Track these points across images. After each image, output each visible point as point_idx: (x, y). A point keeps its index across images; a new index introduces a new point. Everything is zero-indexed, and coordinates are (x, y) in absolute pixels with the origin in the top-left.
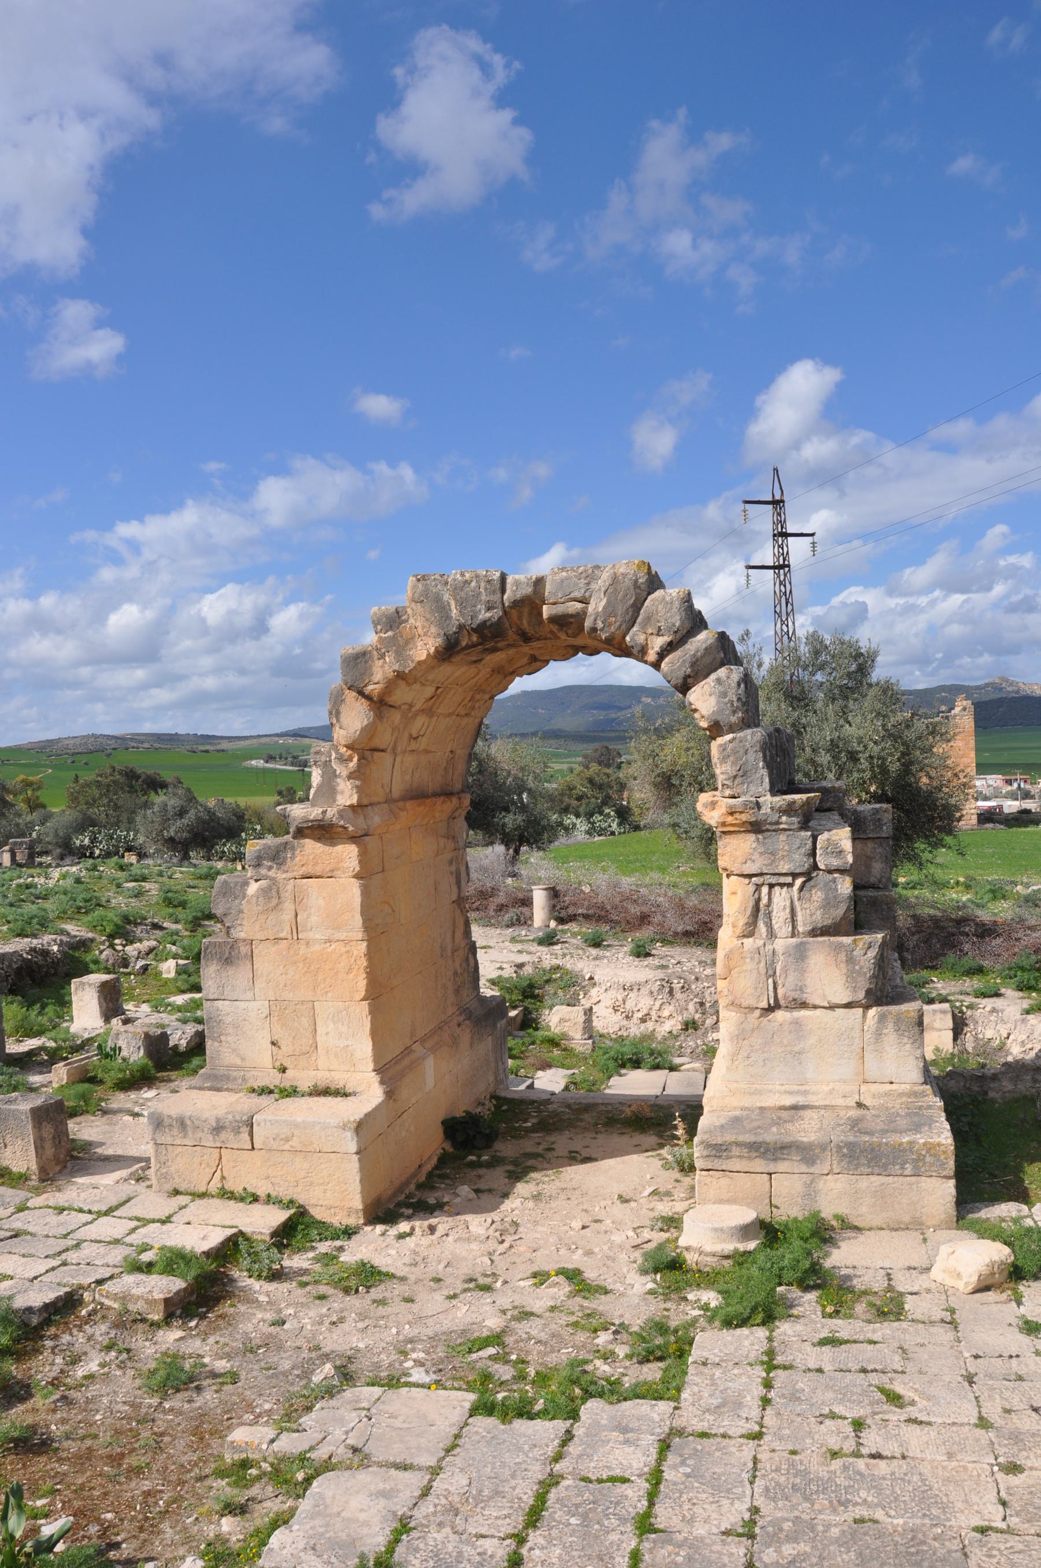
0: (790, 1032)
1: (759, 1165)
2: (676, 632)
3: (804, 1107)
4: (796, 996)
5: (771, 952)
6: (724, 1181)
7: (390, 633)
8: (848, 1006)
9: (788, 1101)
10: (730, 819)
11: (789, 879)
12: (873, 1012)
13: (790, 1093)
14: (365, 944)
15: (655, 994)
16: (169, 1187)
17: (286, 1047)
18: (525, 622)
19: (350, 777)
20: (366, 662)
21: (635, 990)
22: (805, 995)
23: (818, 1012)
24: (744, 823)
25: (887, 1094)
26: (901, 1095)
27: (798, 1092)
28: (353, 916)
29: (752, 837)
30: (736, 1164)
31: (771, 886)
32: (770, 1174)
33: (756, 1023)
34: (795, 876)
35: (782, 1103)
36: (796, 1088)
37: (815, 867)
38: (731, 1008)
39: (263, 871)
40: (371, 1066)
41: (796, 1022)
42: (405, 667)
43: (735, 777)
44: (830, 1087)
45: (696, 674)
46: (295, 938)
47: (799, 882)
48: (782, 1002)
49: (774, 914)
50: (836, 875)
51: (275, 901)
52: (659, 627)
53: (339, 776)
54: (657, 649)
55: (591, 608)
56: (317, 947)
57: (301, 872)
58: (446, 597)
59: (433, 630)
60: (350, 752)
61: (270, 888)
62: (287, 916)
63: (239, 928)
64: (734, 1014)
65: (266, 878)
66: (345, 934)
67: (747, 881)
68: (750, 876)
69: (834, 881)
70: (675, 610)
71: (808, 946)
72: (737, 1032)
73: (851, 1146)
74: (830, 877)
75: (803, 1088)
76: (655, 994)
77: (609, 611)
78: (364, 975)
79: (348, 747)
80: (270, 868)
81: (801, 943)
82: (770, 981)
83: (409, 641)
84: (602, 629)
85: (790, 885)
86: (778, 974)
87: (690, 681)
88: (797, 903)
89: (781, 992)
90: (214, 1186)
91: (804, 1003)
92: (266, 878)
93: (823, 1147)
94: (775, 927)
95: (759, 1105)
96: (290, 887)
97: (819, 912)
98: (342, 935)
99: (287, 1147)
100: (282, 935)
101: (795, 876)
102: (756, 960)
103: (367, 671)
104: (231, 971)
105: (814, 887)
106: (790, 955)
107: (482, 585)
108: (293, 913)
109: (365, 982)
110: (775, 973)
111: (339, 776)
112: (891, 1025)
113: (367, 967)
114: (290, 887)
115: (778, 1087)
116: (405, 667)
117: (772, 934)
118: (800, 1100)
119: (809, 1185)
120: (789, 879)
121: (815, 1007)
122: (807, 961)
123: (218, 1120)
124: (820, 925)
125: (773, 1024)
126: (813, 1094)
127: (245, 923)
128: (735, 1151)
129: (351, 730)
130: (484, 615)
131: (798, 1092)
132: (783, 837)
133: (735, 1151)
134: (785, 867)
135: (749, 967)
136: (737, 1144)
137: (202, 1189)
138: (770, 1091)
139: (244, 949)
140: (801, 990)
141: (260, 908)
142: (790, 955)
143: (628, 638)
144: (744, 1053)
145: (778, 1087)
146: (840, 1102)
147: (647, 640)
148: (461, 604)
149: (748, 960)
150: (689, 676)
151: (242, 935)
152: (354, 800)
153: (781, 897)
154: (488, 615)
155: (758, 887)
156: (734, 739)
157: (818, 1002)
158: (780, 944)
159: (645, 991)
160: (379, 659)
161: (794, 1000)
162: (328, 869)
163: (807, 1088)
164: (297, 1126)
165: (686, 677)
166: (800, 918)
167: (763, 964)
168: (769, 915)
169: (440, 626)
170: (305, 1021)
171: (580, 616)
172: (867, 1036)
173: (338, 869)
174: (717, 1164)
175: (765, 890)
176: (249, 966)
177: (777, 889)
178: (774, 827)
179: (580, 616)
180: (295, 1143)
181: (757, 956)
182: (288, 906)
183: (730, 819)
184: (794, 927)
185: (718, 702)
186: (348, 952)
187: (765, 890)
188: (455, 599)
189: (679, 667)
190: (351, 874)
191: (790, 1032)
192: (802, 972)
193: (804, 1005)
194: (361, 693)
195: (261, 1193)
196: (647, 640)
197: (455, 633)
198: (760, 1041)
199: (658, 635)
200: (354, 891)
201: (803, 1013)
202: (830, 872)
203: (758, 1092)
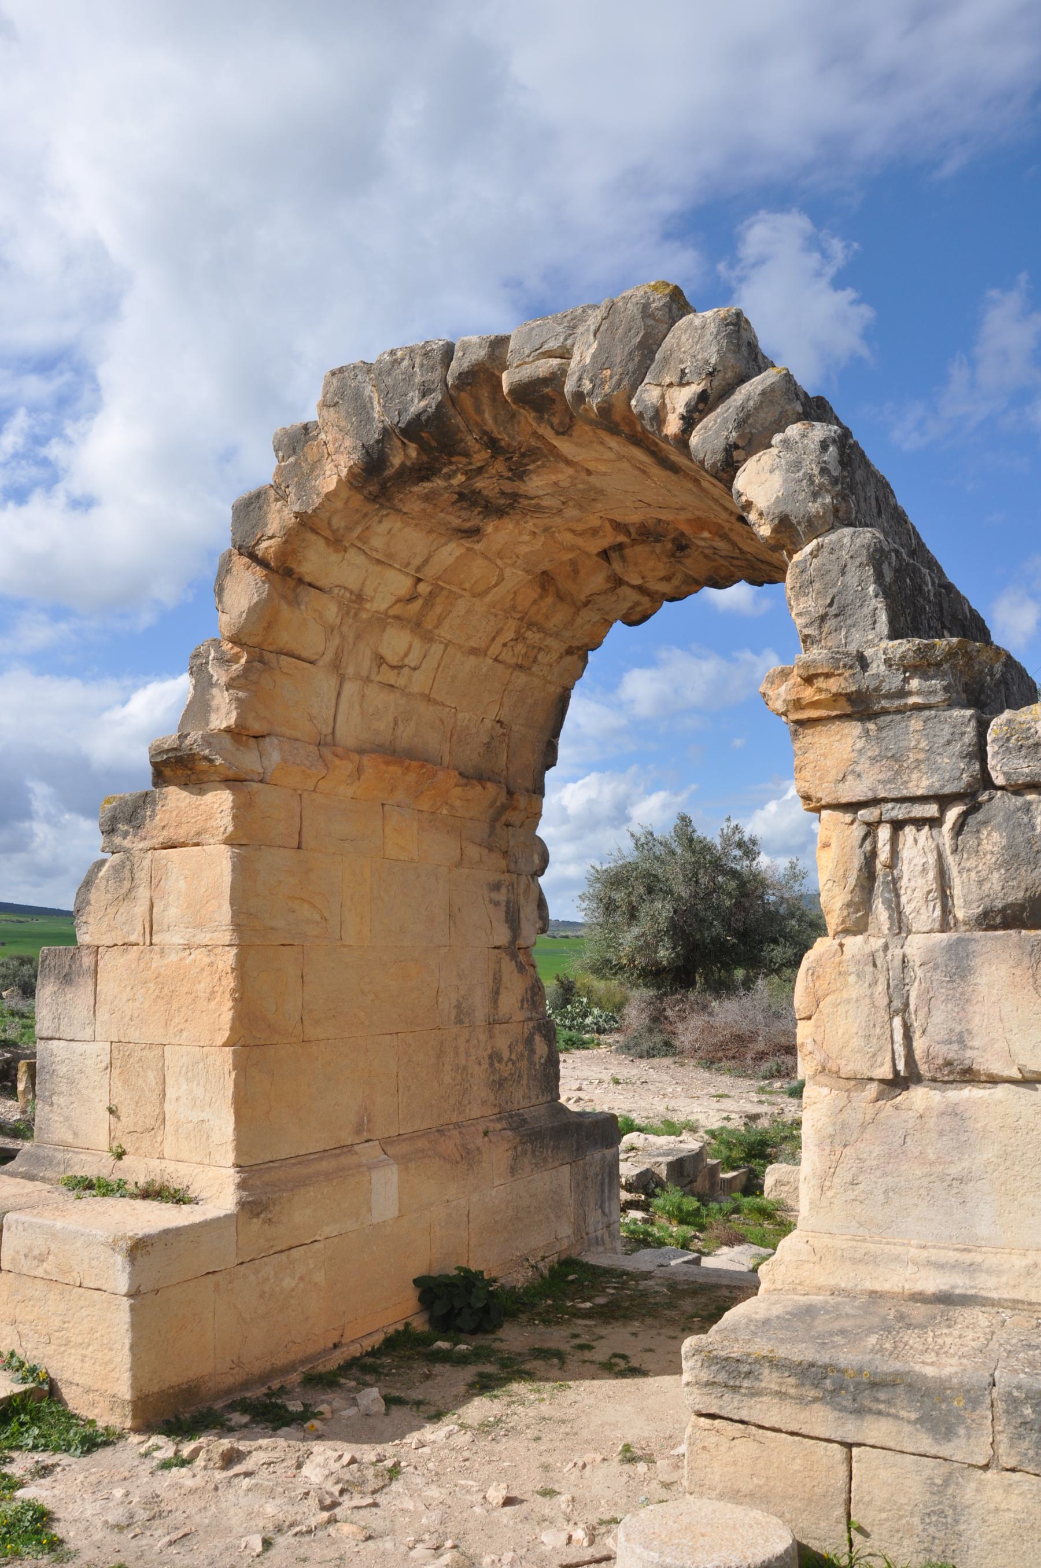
0: (941, 1133)
2: (710, 374)
4: (951, 1056)
5: (897, 962)
6: (745, 1448)
7: (292, 459)
9: (932, 1283)
10: (808, 694)
11: (931, 810)
13: (940, 1266)
14: (234, 951)
17: (127, 1120)
18: (487, 416)
19: (229, 687)
20: (260, 508)
22: (969, 1053)
23: (1001, 1091)
24: (837, 696)
27: (955, 1266)
28: (220, 906)
29: (854, 729)
31: (898, 826)
32: (849, 1446)
33: (871, 1110)
34: (944, 801)
35: (918, 1287)
36: (952, 1256)
37: (985, 781)
38: (821, 1078)
39: (117, 840)
40: (230, 1158)
41: (953, 1112)
42: (308, 504)
43: (823, 618)
44: (1029, 1260)
45: (750, 441)
46: (148, 942)
47: (953, 814)
48: (923, 1068)
49: (904, 883)
50: (1030, 797)
51: (127, 884)
52: (683, 371)
53: (216, 685)
54: (681, 409)
55: (573, 363)
57: (161, 839)
58: (369, 390)
60: (236, 649)
61: (122, 864)
62: (141, 909)
64: (826, 1091)
66: (209, 936)
67: (848, 817)
69: (1027, 808)
70: (708, 337)
71: (972, 947)
72: (830, 1130)
74: (1019, 801)
75: (968, 1258)
77: (602, 360)
78: (230, 1004)
79: (235, 640)
80: (125, 835)
81: (959, 941)
82: (897, 1021)
84: (591, 393)
85: (935, 823)
86: (912, 1007)
87: (737, 455)
88: (951, 860)
89: (919, 1045)
91: (969, 1071)
94: (908, 910)
95: (868, 1285)
96: (146, 863)
97: (996, 875)
98: (204, 938)
99: (39, 1272)
100: (133, 938)
102: (869, 978)
103: (262, 521)
105: (985, 823)
106: (936, 967)
108: (148, 903)
109: (231, 1013)
110: (907, 1005)
111: (216, 685)
113: (234, 991)
114: (146, 863)
115: (914, 1252)
116: (308, 504)
117: (900, 926)
118: (958, 1283)
120: (931, 810)
121: (994, 1080)
122: (972, 979)
124: (999, 904)
125: (905, 1115)
126: (989, 1272)
127: (90, 920)
129: (235, 613)
130: (417, 405)
131: (955, 1266)
132: (915, 723)
133: (769, 1379)
134: (921, 784)
135: (853, 993)
138: (897, 1258)
139: (87, 961)
140: (961, 1041)
141: (109, 896)
142: (936, 967)
143: (633, 402)
144: (844, 1175)
145: (914, 1252)
147: (663, 397)
148: (386, 394)
149: (852, 979)
150: (736, 446)
152: (231, 720)
154: (423, 404)
155: (871, 828)
156: (820, 547)
157: (997, 1068)
158: (916, 946)
160: (277, 500)
161: (948, 1063)
162: (192, 833)
163: (978, 1258)
165: (730, 449)
166: (957, 890)
167: (881, 987)
170: (152, 1076)
171: (556, 379)
174: (729, 1405)
175: (884, 833)
176: (90, 982)
177: (909, 831)
178: (897, 703)
179: (556, 379)
181: (870, 968)
182: (143, 893)
183: (808, 694)
184: (946, 910)
185: (785, 481)
186: (211, 964)
187: (884, 833)
189: (717, 433)
190: (221, 837)
191: (941, 1133)
192: (963, 1002)
193: (969, 1076)
194: (252, 556)
196: (663, 397)
197: (378, 442)
198: (877, 1151)
199: (682, 384)
202: (1018, 789)
203: (870, 1259)
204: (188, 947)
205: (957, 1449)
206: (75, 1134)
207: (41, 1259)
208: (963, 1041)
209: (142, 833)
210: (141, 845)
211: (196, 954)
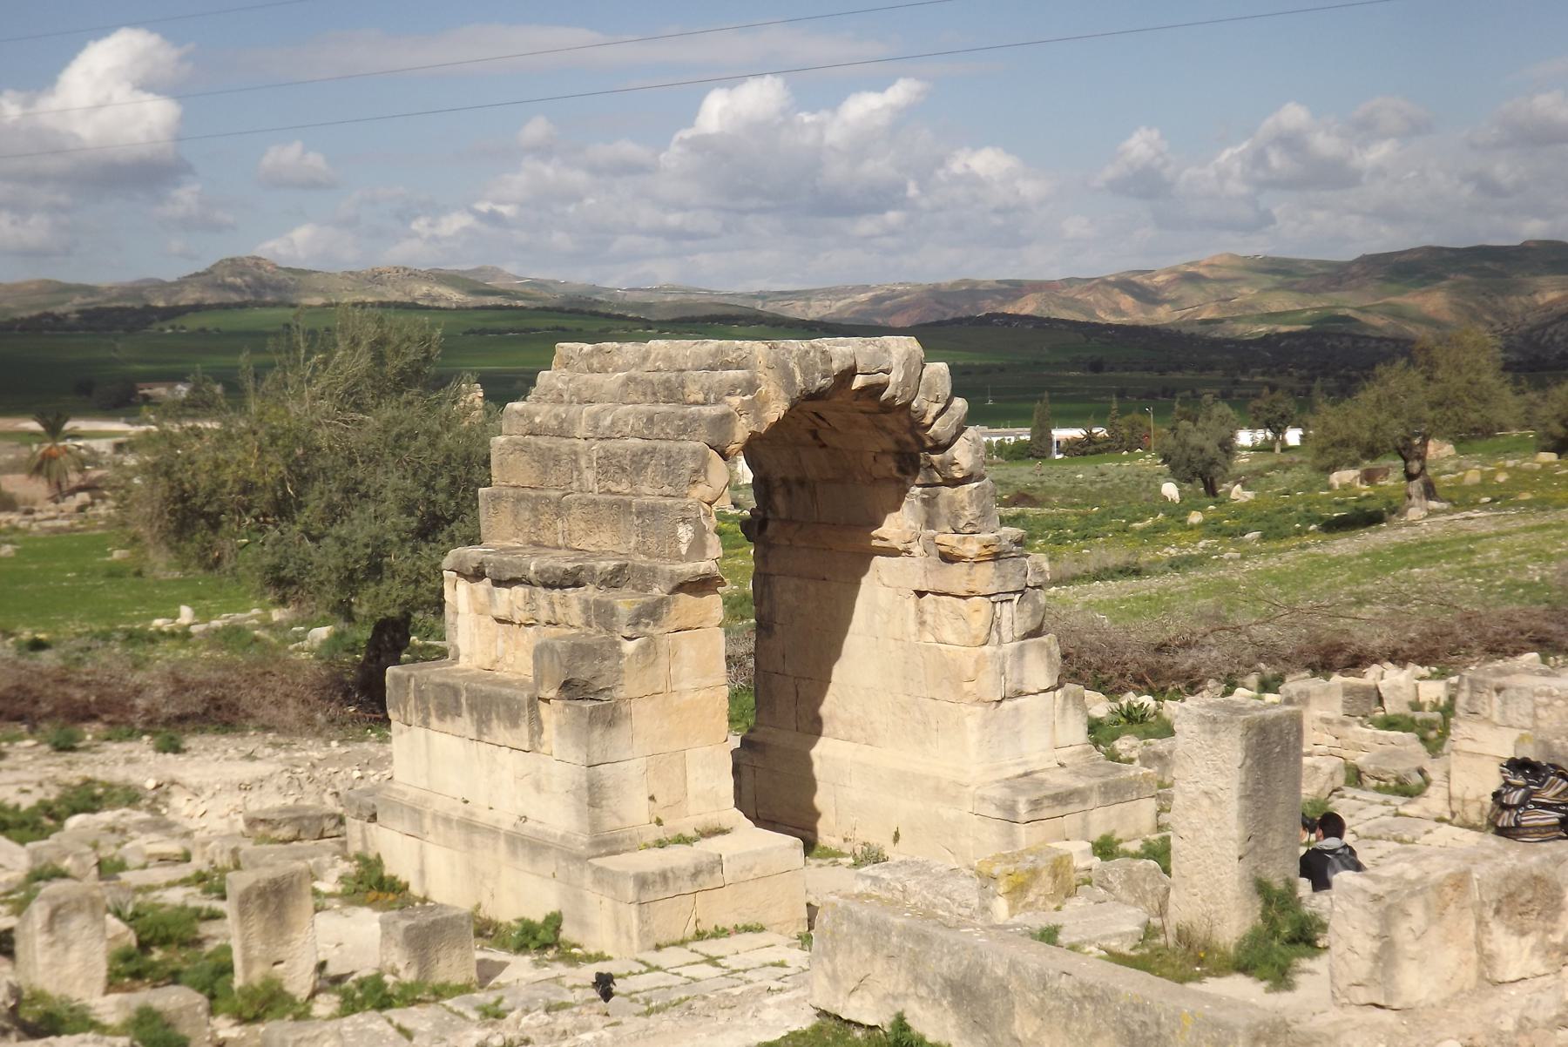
1: (1058, 811)
3: (1031, 773)
6: (1040, 828)
7: (749, 397)
8: (1046, 691)
9: (1021, 771)
12: (1059, 693)
13: (1018, 764)
15: (285, 788)
16: (652, 943)
17: (661, 800)
21: (256, 788)
25: (1071, 755)
26: (1079, 753)
30: (1046, 813)
39: (641, 628)
51: (652, 657)
56: (688, 697)
58: (791, 365)
59: (783, 394)
63: (619, 688)
65: (644, 635)
68: (988, 596)
69: (1037, 594)
73: (1105, 785)
76: (285, 788)
77: (906, 382)
80: (647, 625)
81: (1022, 646)
83: (766, 403)
85: (1011, 600)
90: (690, 931)
92: (644, 635)
93: (1091, 789)
98: (709, 682)
99: (751, 876)
100: (658, 690)
101: (1015, 592)
103: (730, 433)
104: (614, 732)
107: (818, 354)
112: (1070, 701)
114: (664, 642)
117: (1000, 641)
119: (1084, 820)
120: (1011, 596)
123: (696, 867)
127: (625, 682)
128: (1046, 803)
132: (1010, 563)
133: (1046, 803)
136: (1046, 797)
137: (680, 938)
143: (915, 404)
146: (1047, 765)
148: (804, 372)
151: (623, 695)
153: (1006, 611)
154: (823, 382)
159: (269, 788)
164: (758, 854)
166: (1016, 626)
168: (999, 626)
169: (787, 392)
172: (1057, 712)
173: (706, 619)
179: (883, 387)
180: (757, 871)
183: (984, 551)
188: (801, 369)
192: (1021, 667)
193: (1020, 694)
195: (729, 926)
200: (717, 643)
201: (1019, 700)
203: (999, 768)
204: (697, 690)
205: (1088, 807)
206: (621, 819)
207: (750, 870)
208: (1021, 681)
209: (660, 623)
210: (660, 631)
211: (702, 693)
